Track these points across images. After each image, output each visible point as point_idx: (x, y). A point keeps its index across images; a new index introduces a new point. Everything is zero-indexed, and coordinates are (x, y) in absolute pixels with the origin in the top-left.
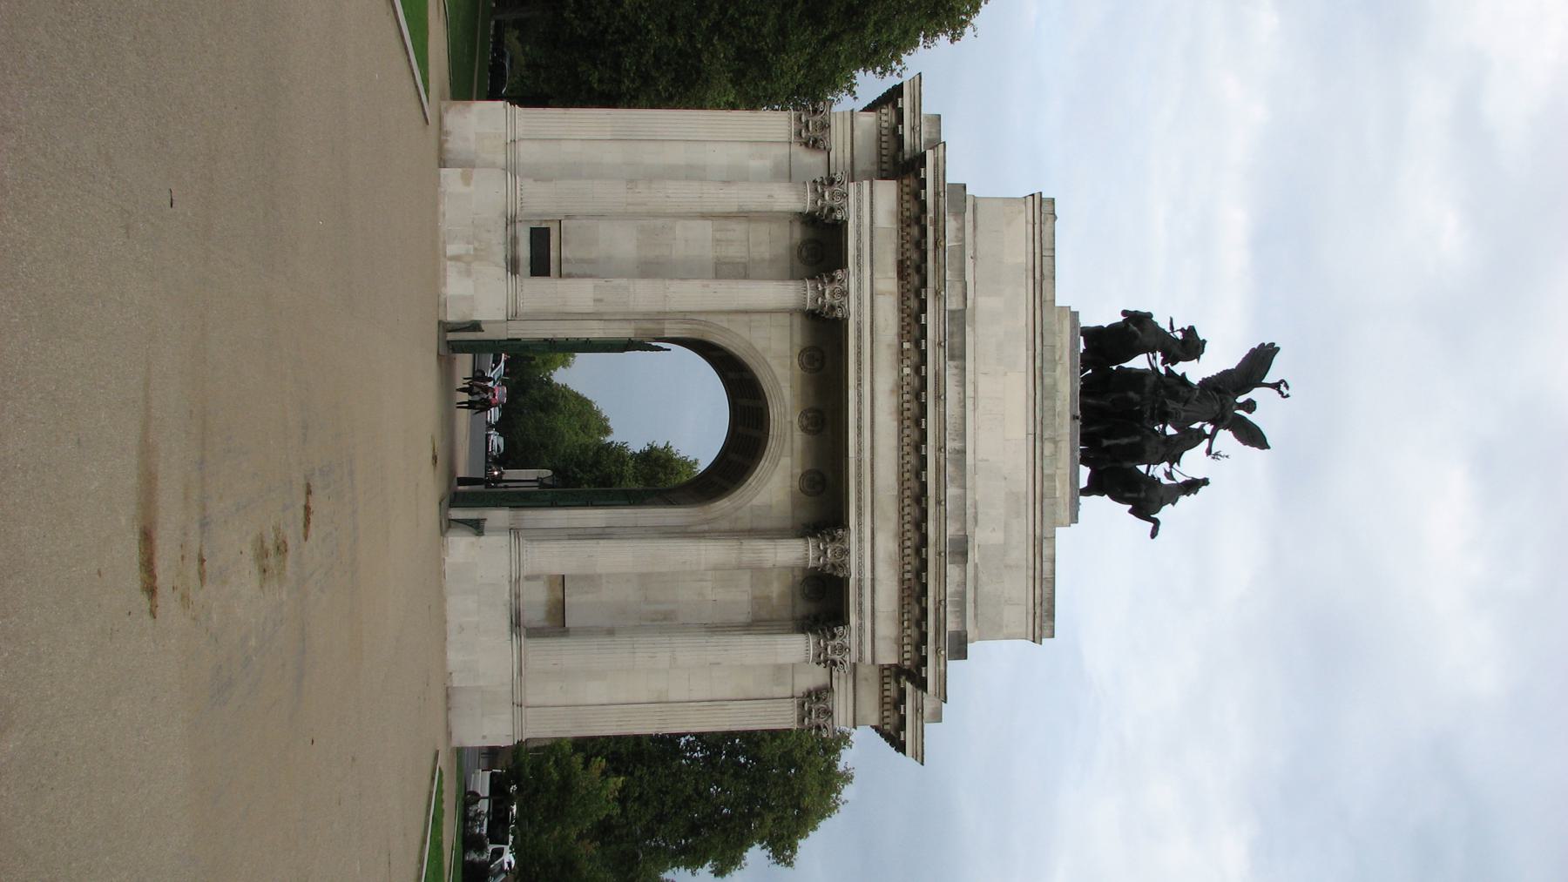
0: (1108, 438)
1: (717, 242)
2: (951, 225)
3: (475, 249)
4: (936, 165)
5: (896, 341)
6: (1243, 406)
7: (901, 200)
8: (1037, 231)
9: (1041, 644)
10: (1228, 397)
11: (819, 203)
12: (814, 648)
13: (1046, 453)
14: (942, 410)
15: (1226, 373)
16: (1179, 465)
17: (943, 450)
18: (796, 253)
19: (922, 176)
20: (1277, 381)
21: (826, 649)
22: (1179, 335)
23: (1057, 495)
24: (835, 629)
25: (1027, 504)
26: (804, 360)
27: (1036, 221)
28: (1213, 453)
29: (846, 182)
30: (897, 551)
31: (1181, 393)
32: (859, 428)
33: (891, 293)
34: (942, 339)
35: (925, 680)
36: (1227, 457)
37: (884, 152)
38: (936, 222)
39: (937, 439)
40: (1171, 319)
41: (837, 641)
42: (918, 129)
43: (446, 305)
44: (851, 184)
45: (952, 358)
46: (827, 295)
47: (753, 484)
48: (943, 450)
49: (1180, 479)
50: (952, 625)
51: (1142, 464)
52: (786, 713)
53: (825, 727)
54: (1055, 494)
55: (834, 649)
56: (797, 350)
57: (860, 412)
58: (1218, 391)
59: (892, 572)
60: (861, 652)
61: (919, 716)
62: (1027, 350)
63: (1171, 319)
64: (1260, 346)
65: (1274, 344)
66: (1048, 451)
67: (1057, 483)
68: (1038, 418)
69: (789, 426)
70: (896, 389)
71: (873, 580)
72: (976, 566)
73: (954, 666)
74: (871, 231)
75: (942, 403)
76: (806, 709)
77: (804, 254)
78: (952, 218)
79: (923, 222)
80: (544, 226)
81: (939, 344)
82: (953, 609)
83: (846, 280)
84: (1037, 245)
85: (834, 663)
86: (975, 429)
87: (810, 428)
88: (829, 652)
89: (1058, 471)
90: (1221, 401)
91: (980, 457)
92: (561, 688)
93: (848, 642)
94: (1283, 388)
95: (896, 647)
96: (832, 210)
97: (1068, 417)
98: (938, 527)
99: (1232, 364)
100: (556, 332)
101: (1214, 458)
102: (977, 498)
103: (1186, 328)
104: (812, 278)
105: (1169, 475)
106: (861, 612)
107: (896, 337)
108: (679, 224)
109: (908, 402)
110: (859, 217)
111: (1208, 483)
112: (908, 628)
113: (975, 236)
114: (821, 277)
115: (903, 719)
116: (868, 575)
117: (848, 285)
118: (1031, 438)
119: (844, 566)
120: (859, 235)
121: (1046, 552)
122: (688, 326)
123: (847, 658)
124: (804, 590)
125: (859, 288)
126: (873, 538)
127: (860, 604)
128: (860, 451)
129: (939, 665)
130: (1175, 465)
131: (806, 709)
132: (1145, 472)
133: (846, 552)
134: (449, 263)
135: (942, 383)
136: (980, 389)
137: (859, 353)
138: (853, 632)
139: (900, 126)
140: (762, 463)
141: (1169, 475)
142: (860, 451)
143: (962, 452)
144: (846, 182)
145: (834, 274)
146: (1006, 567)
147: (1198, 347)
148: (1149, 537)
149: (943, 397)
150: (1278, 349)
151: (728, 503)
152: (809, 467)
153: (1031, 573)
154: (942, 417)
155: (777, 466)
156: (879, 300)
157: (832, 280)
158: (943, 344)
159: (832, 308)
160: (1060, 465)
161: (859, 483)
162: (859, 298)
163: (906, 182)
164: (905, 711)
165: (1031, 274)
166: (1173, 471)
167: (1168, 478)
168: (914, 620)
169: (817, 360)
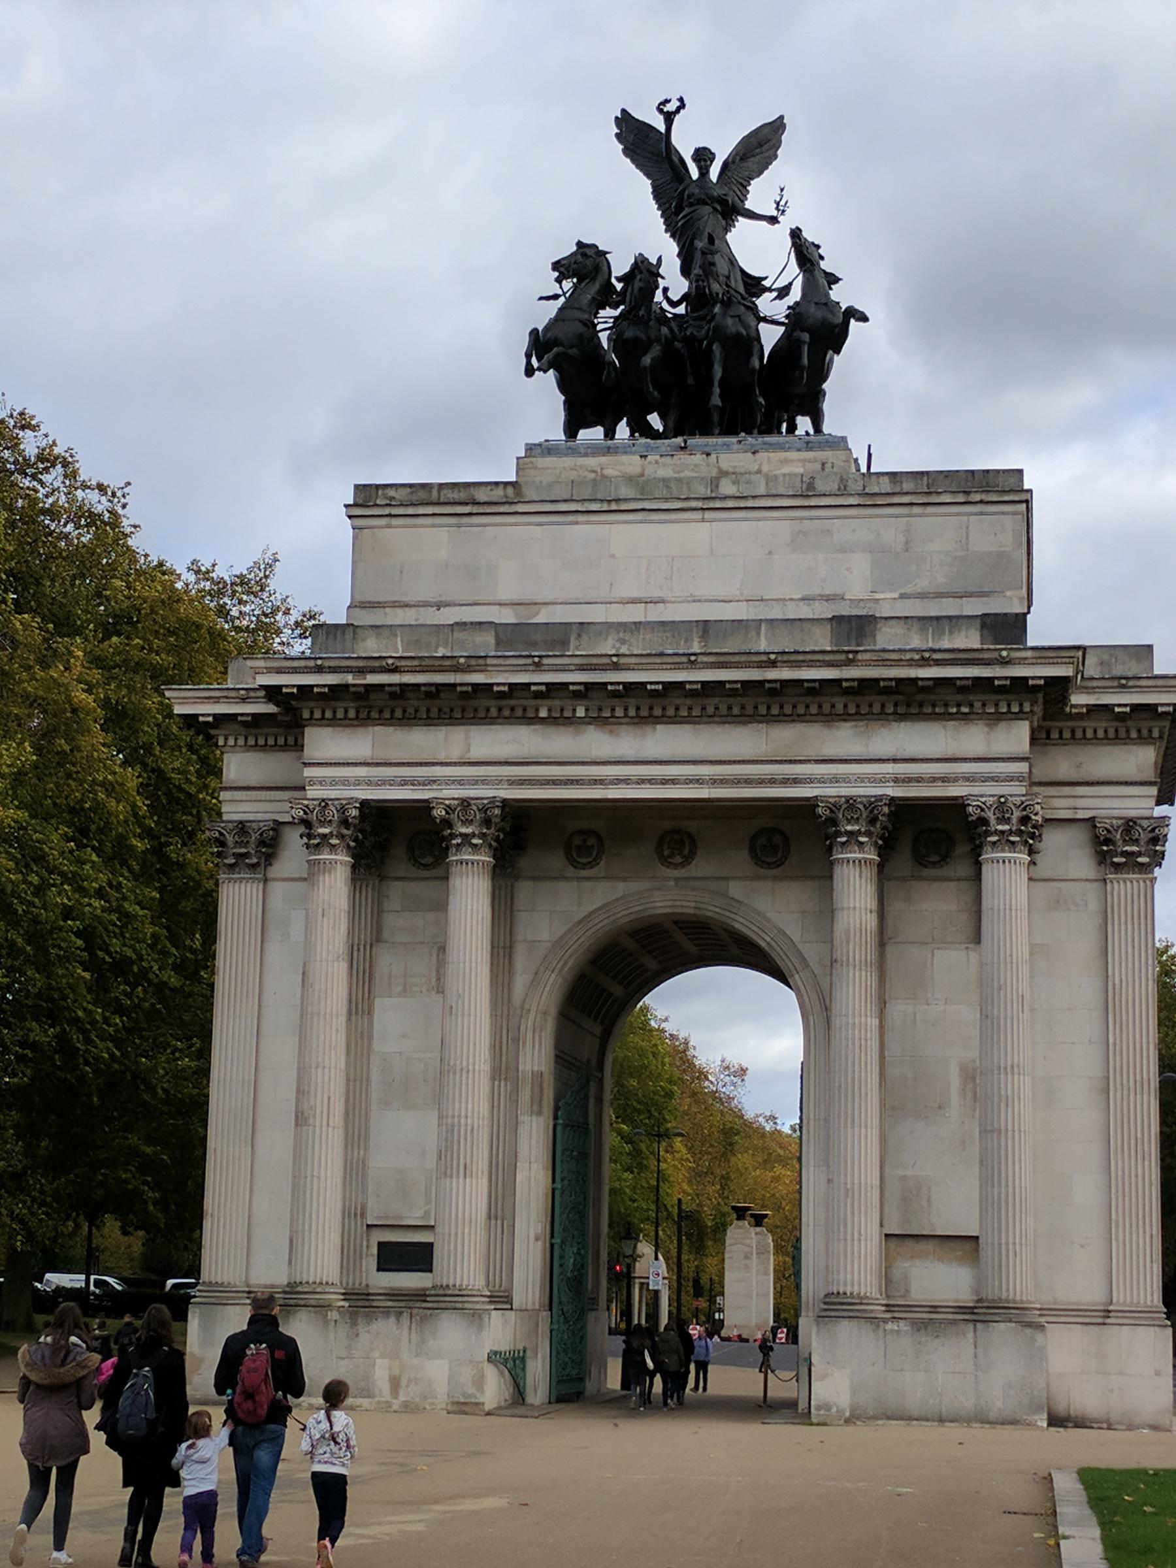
0: (709, 395)
1: (405, 991)
2: (371, 647)
3: (382, 1356)
4: (280, 671)
6: (704, 172)
7: (334, 722)
8: (401, 511)
9: (1030, 491)
10: (686, 192)
11: (334, 841)
12: (1003, 851)
14: (633, 660)
15: (658, 195)
16: (766, 278)
17: (693, 658)
18: (426, 873)
19: (295, 690)
20: (661, 118)
21: (1003, 832)
22: (568, 285)
23: (801, 470)
24: (970, 819)
25: (811, 519)
26: (583, 860)
27: (387, 511)
28: (775, 213)
29: (306, 802)
30: (854, 723)
31: (641, 284)
32: (665, 782)
33: (467, 738)
34: (529, 661)
35: (1051, 681)
36: (782, 190)
37: (281, 741)
38: (361, 671)
39: (677, 666)
40: (541, 298)
41: (990, 815)
42: (242, 692)
43: (464, 1403)
44: (311, 793)
45: (565, 643)
46: (469, 830)
47: (768, 939)
48: (693, 658)
49: (794, 271)
50: (969, 639)
51: (758, 339)
52: (1129, 891)
53: (1153, 830)
54: (796, 475)
55: (1002, 820)
56: (570, 871)
57: (642, 781)
58: (679, 209)
59: (884, 731)
60: (1010, 779)
61: (1131, 683)
62: (577, 523)
63: (541, 298)
64: (620, 141)
65: (617, 118)
66: (727, 488)
67: (786, 470)
68: (680, 505)
70: (609, 727)
71: (895, 761)
72: (903, 596)
73: (1038, 633)
74: (378, 764)
75: (623, 660)
76: (1123, 860)
77: (428, 860)
78: (361, 645)
79: (362, 689)
80: (375, 1251)
81: (537, 664)
82: (946, 637)
83: (447, 802)
84: (421, 510)
85: (1025, 820)
86: (694, 601)
87: (686, 852)
88: (1007, 827)
89: (765, 469)
90: (691, 205)
91: (738, 593)
92: (1082, 1246)
93: (991, 799)
94: (671, 107)
95: (1003, 725)
96: (345, 822)
97: (683, 458)
98: (811, 664)
99: (646, 184)
100: (532, 1237)
101: (783, 211)
102: (799, 596)
103: (556, 274)
104: (445, 852)
105: (784, 292)
106: (945, 779)
107: (532, 727)
108: (377, 1046)
109: (626, 710)
110: (358, 782)
111: (798, 228)
112: (971, 706)
113: (407, 606)
114: (444, 839)
115: (1136, 708)
116: (889, 768)
117: (454, 799)
118: (708, 515)
119: (872, 804)
120: (382, 783)
121: (885, 485)
122: (530, 1034)
123: (1018, 800)
124: (934, 863)
125: (460, 782)
126: (832, 761)
127: (934, 779)
128: (698, 781)
129: (1026, 659)
130: (767, 283)
131: (1123, 860)
132: (783, 329)
133: (851, 802)
134: (402, 1398)
135: (594, 661)
136: (634, 594)
138: (976, 790)
139: (240, 718)
140: (737, 925)
141: (784, 292)
142: (698, 781)
143: (705, 627)
144: (306, 802)
145: (438, 821)
146: (907, 550)
147: (584, 255)
148: (867, 324)
149: (615, 659)
150: (624, 111)
151: (797, 976)
152: (745, 855)
153: (917, 510)
154: (644, 660)
155: (741, 903)
156: (477, 753)
157: (448, 823)
158: (536, 660)
159: (487, 822)
160: (756, 468)
161: (748, 782)
163: (306, 715)
164: (1125, 705)
165: (465, 520)
166: (773, 287)
167: (787, 294)
168: (959, 697)
169: (584, 841)
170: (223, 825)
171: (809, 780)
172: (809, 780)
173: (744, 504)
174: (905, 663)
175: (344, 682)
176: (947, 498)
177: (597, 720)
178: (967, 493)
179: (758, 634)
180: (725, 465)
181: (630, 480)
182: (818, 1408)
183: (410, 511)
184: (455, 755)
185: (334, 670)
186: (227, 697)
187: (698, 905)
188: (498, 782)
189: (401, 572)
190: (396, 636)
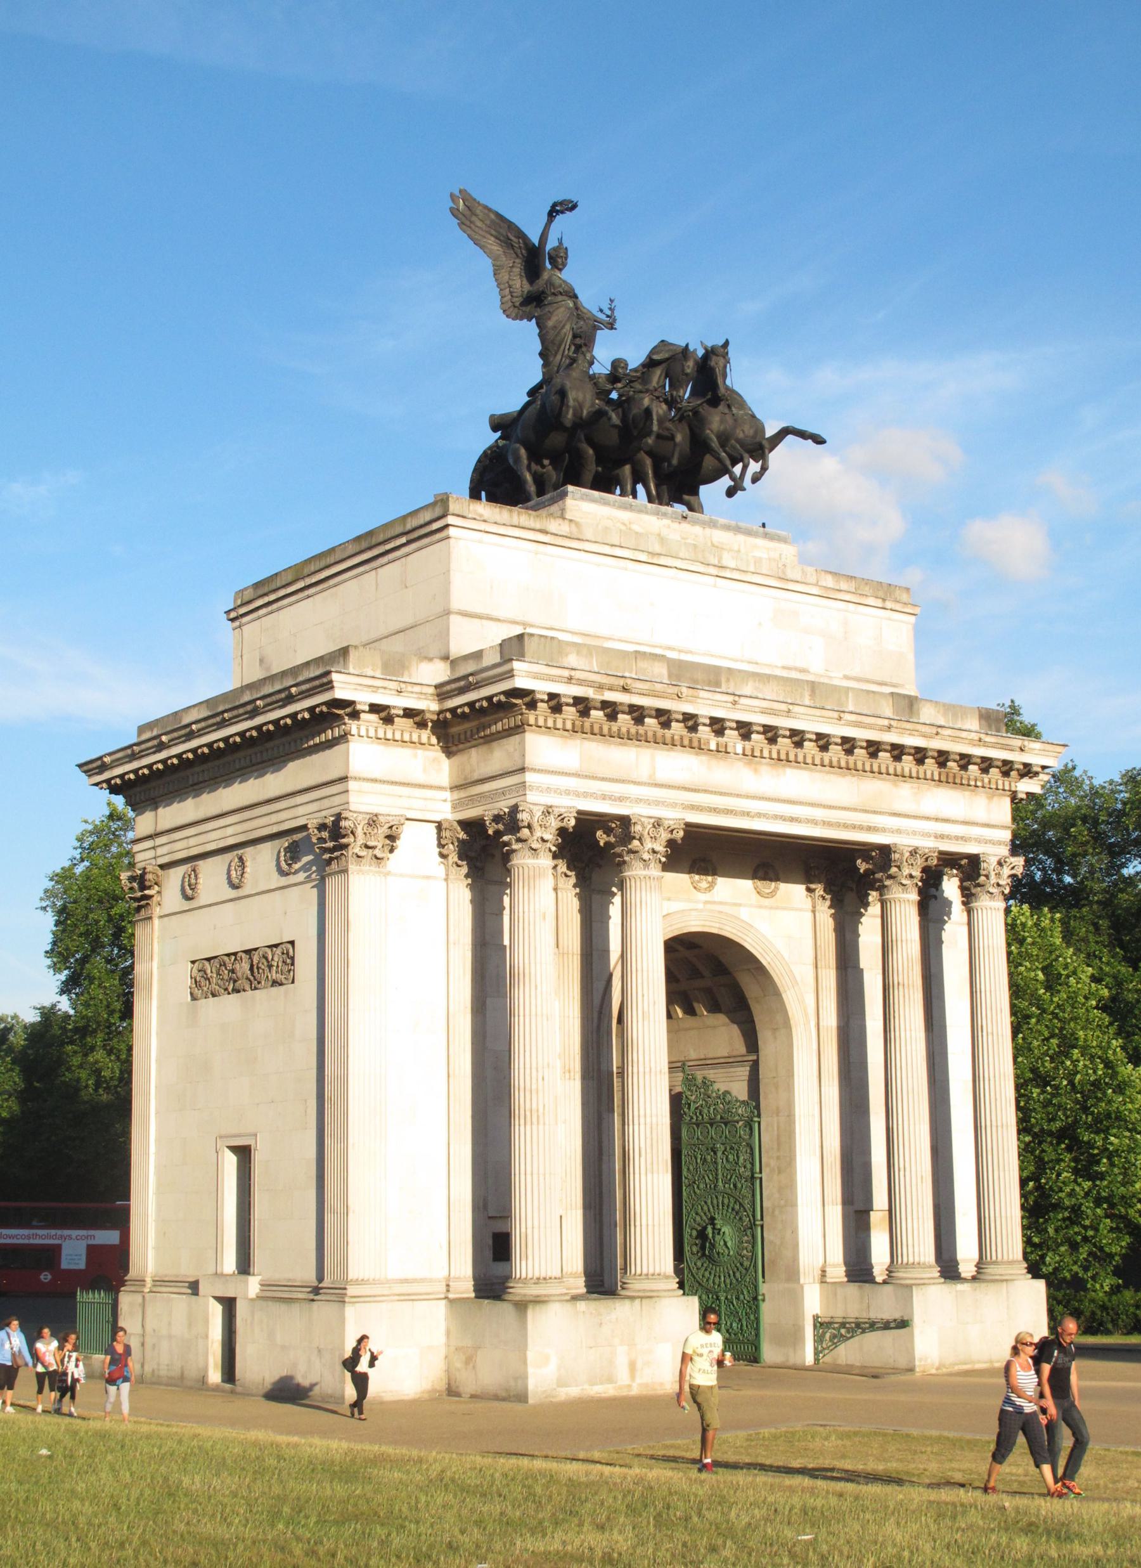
4: (537, 676)
5: (704, 758)
8: (494, 529)
13: (732, 564)
17: (842, 715)
32: (792, 819)
34: (730, 698)
36: (612, 301)
45: (718, 684)
47: (769, 960)
57: (776, 817)
60: (1000, 843)
66: (728, 560)
67: (757, 554)
69: (709, 906)
71: (937, 820)
72: (846, 677)
74: (586, 777)
75: (796, 709)
81: (735, 703)
101: (615, 320)
110: (568, 792)
113: (499, 620)
120: (586, 795)
125: (648, 802)
127: (957, 838)
128: (814, 822)
134: (638, 1381)
137: (715, 810)
142: (814, 822)
149: (791, 707)
156: (662, 776)
159: (671, 843)
160: (736, 548)
162: (657, 803)
170: (355, 815)
171: (884, 830)
172: (884, 830)
173: (740, 576)
174: (967, 741)
175: (586, 696)
176: (871, 601)
177: (750, 756)
178: (884, 600)
179: (847, 698)
180: (715, 540)
181: (662, 540)
182: (921, 1360)
183: (502, 530)
184: (643, 774)
185: (581, 682)
186: (385, 688)
187: (722, 926)
188: (674, 805)
189: (492, 587)
190: (591, 654)
